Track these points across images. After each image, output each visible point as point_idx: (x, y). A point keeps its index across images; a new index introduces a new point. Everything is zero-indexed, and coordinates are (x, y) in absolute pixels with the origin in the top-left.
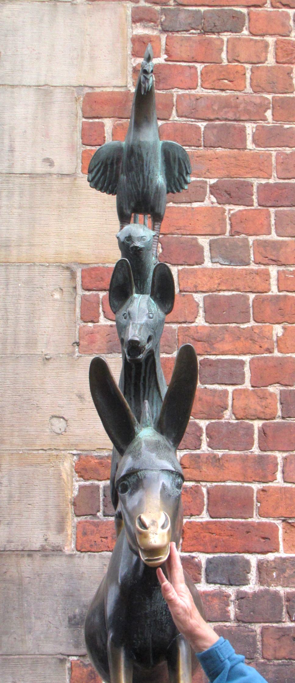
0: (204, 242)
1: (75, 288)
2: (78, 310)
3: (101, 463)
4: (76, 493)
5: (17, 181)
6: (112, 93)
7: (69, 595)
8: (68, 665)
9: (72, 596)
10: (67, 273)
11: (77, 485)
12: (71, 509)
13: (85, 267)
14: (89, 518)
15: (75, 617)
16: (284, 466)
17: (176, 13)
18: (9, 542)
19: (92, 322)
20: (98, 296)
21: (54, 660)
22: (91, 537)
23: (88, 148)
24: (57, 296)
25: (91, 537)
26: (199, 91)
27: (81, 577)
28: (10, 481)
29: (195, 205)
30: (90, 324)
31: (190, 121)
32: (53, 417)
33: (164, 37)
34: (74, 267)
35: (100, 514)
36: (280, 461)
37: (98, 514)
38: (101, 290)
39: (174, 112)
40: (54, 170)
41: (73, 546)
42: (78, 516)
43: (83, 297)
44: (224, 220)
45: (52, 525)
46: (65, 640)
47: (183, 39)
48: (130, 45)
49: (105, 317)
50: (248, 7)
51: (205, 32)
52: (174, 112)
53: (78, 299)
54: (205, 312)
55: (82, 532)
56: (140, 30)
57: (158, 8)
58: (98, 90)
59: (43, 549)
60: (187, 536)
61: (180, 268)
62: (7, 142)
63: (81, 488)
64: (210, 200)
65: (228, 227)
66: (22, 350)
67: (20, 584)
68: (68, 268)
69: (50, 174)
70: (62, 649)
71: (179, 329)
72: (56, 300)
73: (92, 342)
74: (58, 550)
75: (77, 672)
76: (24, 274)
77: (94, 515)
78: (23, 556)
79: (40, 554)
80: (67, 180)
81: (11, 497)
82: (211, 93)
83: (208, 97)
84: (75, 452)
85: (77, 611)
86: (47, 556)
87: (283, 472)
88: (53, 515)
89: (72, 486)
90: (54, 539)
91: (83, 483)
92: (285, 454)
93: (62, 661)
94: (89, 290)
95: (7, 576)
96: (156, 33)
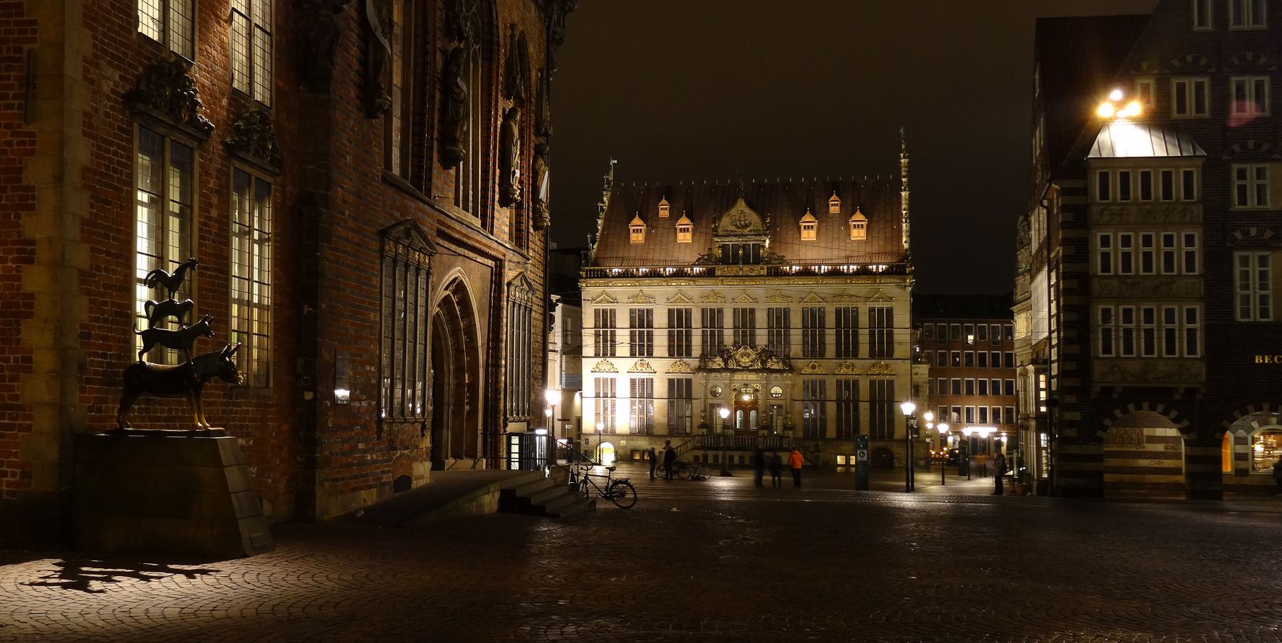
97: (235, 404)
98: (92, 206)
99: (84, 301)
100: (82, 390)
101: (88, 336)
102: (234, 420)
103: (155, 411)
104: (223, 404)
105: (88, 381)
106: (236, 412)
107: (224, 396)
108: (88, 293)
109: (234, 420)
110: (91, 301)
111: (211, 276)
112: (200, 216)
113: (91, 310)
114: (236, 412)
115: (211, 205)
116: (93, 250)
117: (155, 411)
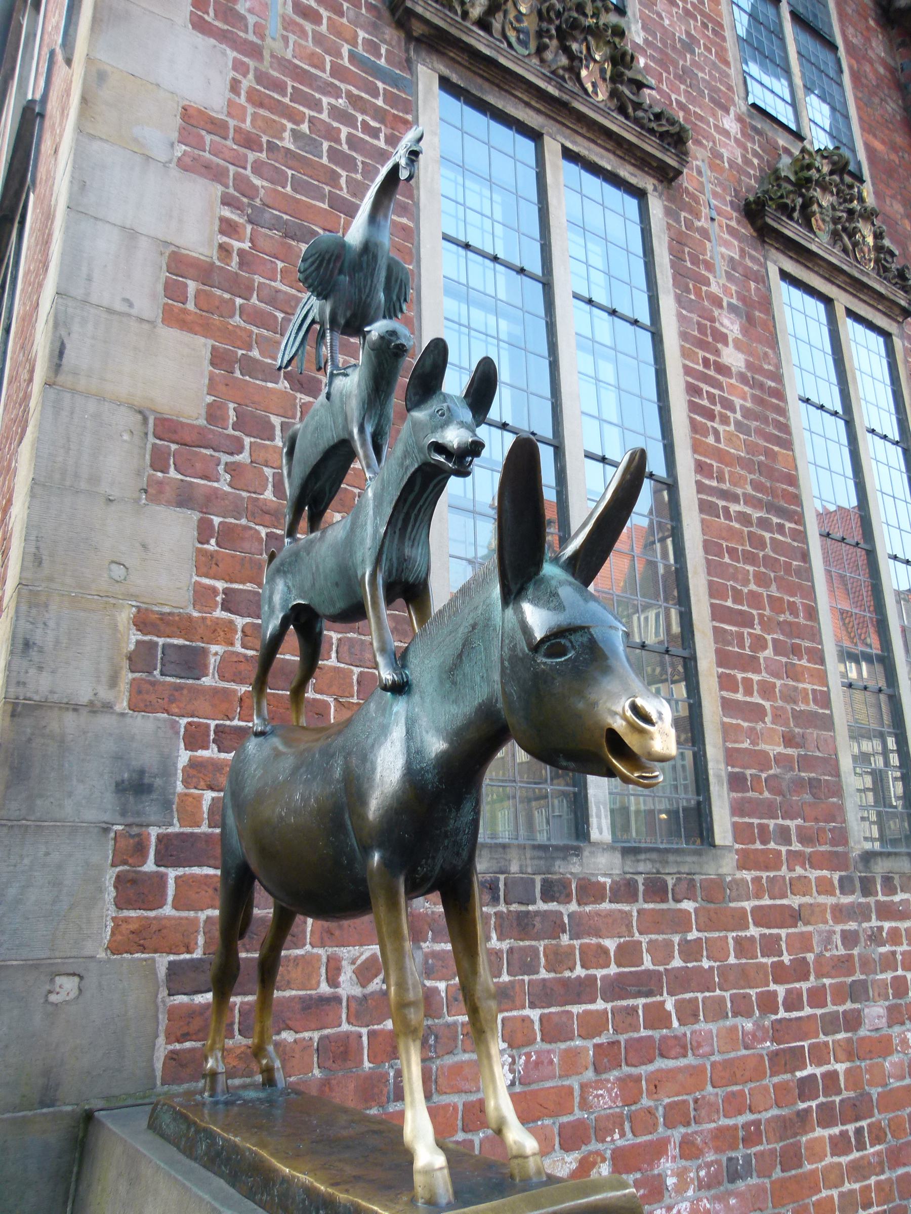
0: (276, 421)
1: (146, 434)
2: (148, 457)
3: (162, 619)
4: (132, 647)
5: (93, 311)
6: (198, 259)
7: (118, 758)
8: (112, 835)
9: (121, 758)
10: (139, 417)
11: (133, 639)
12: (125, 664)
13: (158, 416)
14: (144, 675)
15: (123, 781)
16: (338, 647)
17: (263, 211)
18: (52, 692)
19: (162, 472)
20: (169, 447)
21: (96, 830)
22: (146, 697)
23: (170, 302)
24: (126, 437)
25: (146, 697)
26: (278, 285)
27: (132, 738)
28: (58, 624)
29: (270, 385)
30: (160, 474)
31: (269, 308)
32: (113, 562)
33: (249, 228)
34: (147, 413)
35: (157, 673)
36: (334, 641)
37: (157, 673)
38: (173, 442)
39: (255, 296)
40: (134, 312)
41: (125, 704)
42: (132, 672)
43: (154, 445)
44: (295, 406)
45: (104, 679)
46: (110, 807)
47: (266, 235)
48: (217, 222)
49: (176, 469)
50: (324, 230)
51: (286, 236)
52: (255, 296)
53: (149, 446)
54: (274, 486)
55: (137, 689)
56: (227, 213)
57: (245, 200)
58: (183, 251)
59: (91, 703)
60: (245, 705)
61: (253, 440)
62: (84, 269)
63: (138, 643)
64: (284, 385)
65: (299, 414)
66: (83, 485)
67: (62, 741)
68: (140, 412)
69: (129, 315)
70: (106, 817)
71: (249, 497)
72: (125, 441)
73: (161, 492)
74: (107, 707)
75: (122, 843)
76: (92, 406)
77: (150, 673)
78: (67, 709)
79: (88, 709)
80: (146, 326)
81: (57, 642)
82: (288, 290)
83: (286, 293)
84: (134, 603)
85: (126, 775)
86: (95, 712)
87: (337, 652)
88: (105, 666)
89: (128, 639)
90: (105, 694)
91: (140, 637)
92: (339, 636)
93: (106, 830)
94: (161, 439)
95: (47, 731)
96: (241, 221)
97: (886, 911)
98: (228, 228)
99: (176, 529)
100: (136, 891)
101: (191, 662)
102: (888, 962)
103: (559, 959)
104: (840, 913)
105: (174, 851)
106: (895, 937)
107: (846, 886)
108: (184, 499)
109: (888, 962)
110: (204, 531)
111: (745, 519)
112: (685, 353)
113: (206, 564)
114: (895, 937)
115: (723, 338)
116: (218, 359)
117: (559, 959)
